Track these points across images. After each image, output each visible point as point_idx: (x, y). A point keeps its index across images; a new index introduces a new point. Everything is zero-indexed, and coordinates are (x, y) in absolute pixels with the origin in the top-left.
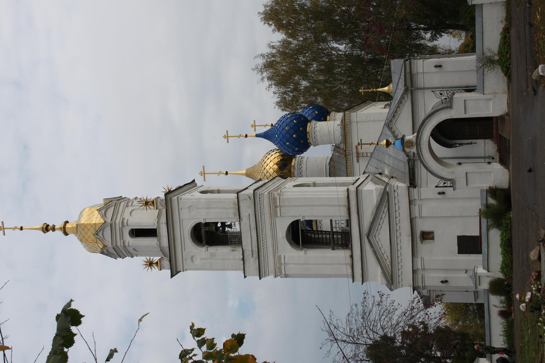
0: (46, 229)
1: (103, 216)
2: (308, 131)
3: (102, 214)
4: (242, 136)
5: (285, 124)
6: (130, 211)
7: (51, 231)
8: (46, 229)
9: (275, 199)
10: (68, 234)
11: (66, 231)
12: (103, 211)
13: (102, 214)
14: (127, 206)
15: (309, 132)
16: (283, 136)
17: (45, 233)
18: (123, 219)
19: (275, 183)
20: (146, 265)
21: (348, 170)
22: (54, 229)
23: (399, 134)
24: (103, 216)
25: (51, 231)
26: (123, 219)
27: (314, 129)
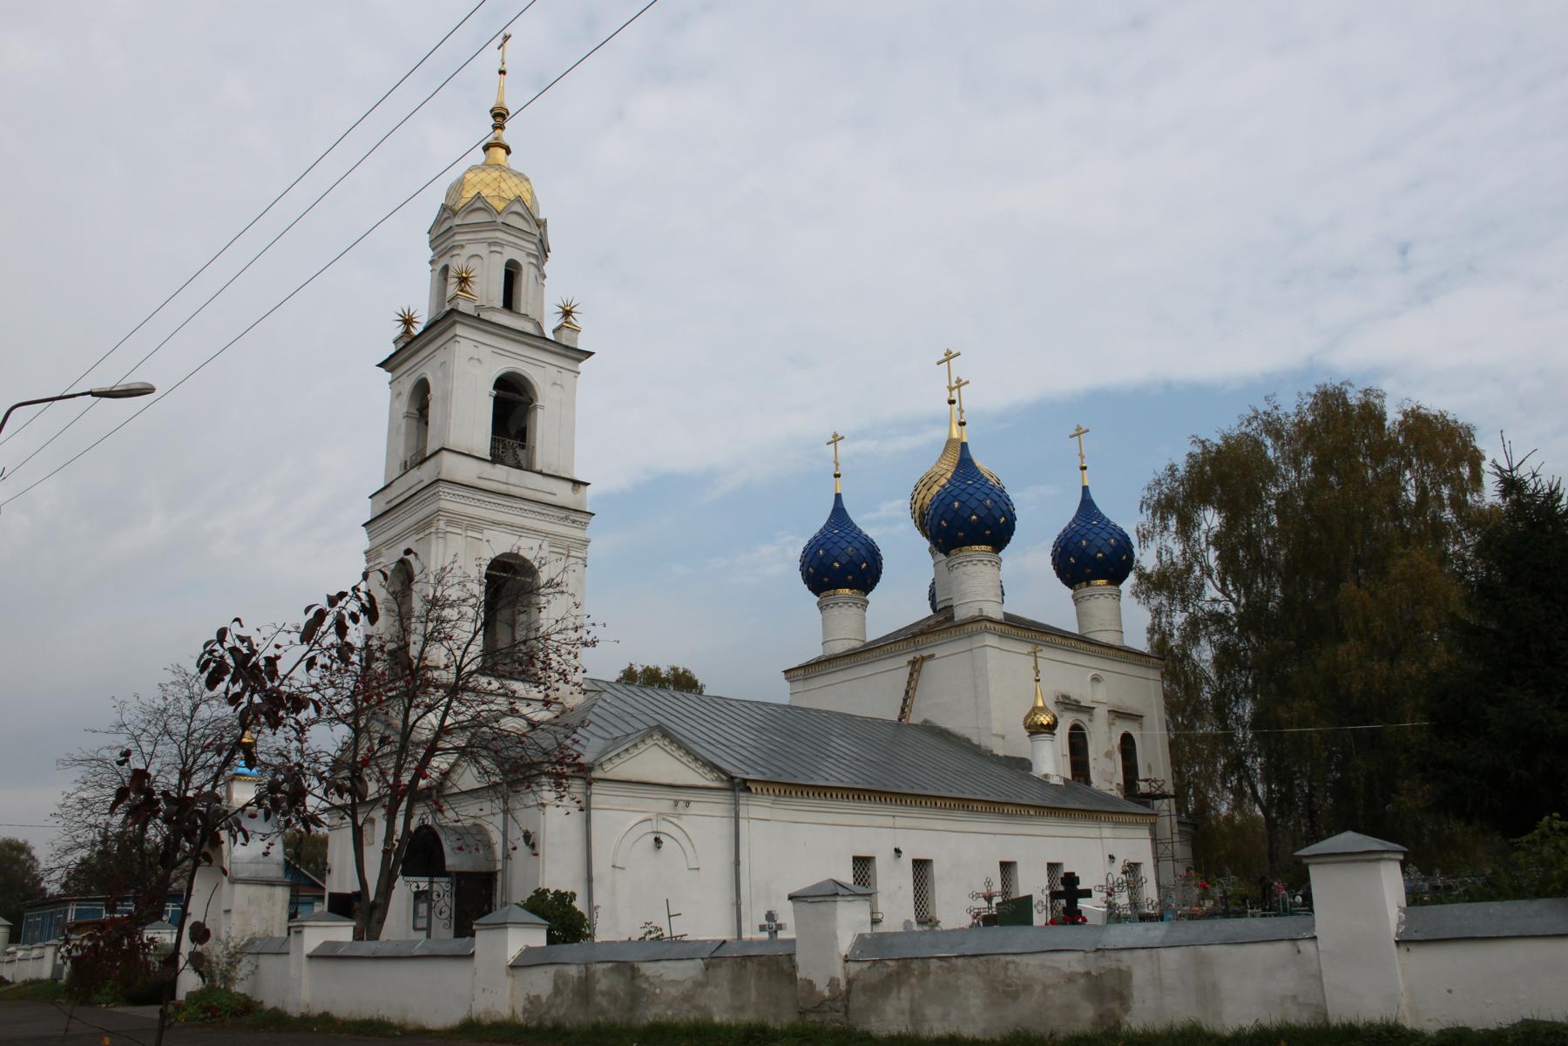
0: (500, 116)
1: (470, 206)
2: (963, 549)
3: (472, 205)
4: (961, 414)
5: (997, 499)
6: (475, 253)
7: (493, 122)
8: (500, 116)
9: (429, 525)
10: (487, 152)
11: (491, 149)
12: (479, 204)
13: (472, 205)
14: (490, 244)
15: (960, 551)
16: (964, 503)
17: (491, 111)
18: (463, 246)
19: (543, 514)
20: (401, 316)
21: (893, 646)
22: (498, 127)
23: (622, 760)
24: (470, 206)
25: (493, 122)
26: (463, 246)
27: (968, 561)
